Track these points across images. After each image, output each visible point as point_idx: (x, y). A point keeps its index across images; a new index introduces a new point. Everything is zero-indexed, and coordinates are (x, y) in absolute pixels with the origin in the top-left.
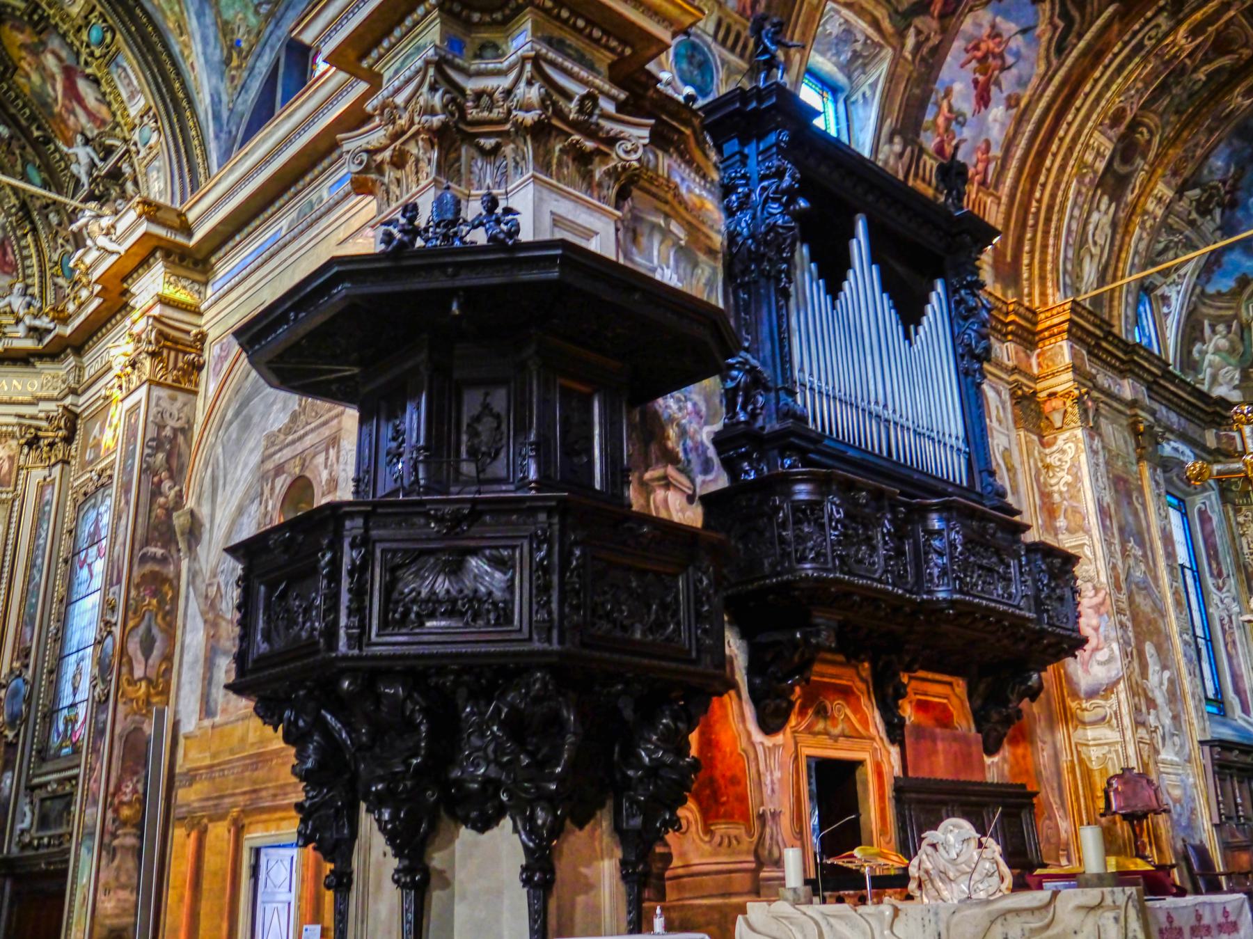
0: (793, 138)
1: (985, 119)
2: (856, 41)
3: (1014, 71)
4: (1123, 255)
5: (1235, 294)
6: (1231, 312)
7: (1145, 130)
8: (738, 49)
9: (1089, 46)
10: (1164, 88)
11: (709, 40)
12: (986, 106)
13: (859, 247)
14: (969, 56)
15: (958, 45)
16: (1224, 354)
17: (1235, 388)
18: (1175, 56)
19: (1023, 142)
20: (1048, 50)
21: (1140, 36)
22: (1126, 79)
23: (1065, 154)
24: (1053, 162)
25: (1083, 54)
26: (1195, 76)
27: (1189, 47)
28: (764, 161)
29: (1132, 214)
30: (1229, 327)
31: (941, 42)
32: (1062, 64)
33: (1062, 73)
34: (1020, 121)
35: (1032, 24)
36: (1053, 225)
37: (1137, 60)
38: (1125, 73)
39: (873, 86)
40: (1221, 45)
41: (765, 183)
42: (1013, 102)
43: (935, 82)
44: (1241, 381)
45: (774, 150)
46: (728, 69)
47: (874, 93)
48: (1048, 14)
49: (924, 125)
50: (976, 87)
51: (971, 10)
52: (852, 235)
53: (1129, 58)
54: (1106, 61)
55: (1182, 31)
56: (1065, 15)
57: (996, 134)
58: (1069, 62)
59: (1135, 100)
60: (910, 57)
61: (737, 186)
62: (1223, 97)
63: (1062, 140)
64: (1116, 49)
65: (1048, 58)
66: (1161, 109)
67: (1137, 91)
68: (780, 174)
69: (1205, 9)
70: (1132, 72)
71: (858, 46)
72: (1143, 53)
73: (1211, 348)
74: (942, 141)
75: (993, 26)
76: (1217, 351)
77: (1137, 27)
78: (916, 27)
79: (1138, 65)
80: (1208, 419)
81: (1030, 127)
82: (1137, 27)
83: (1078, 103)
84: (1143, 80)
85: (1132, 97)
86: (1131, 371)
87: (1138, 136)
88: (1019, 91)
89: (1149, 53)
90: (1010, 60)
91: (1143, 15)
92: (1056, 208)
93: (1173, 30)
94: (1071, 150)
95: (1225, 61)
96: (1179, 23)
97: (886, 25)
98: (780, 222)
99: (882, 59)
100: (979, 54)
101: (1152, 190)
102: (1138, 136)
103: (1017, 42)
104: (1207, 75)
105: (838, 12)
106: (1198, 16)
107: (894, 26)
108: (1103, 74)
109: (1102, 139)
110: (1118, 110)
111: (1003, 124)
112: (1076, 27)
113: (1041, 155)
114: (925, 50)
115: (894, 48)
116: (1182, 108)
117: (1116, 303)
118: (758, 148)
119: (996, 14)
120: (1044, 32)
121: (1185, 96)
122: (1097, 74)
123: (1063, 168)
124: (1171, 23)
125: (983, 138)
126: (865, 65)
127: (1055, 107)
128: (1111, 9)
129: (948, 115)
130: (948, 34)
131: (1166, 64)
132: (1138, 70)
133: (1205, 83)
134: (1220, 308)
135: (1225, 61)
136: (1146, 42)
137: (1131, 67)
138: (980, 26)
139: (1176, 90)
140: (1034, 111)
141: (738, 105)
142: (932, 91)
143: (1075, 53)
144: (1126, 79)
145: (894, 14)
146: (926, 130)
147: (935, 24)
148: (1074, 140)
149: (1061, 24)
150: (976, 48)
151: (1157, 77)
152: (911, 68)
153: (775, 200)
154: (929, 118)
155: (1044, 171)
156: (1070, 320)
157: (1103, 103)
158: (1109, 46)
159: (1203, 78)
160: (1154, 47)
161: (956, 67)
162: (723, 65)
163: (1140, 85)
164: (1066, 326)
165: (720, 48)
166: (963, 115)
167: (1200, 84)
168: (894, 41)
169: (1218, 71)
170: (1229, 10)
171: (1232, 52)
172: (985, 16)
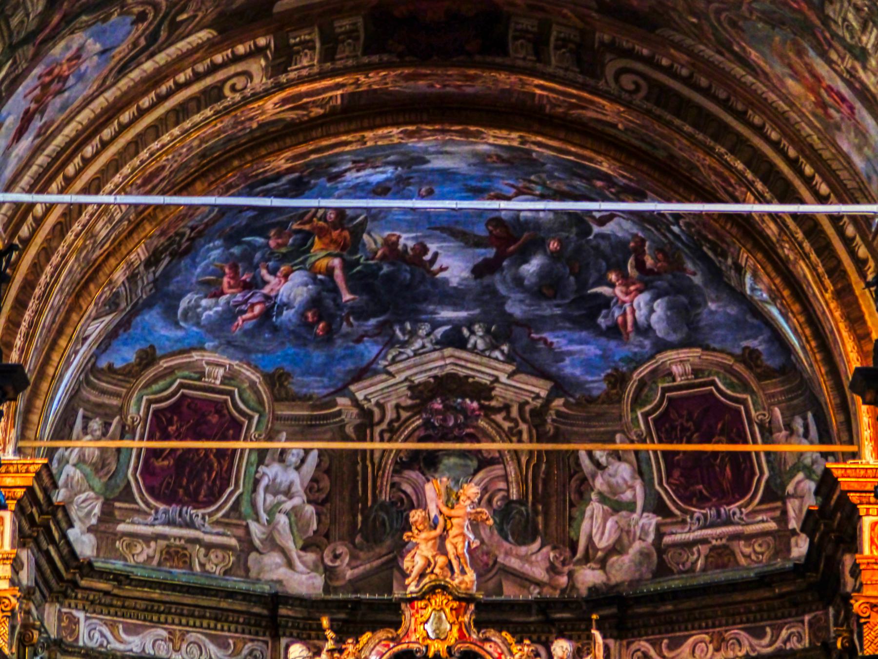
4: (63, 342)
5: (130, 374)
6: (115, 402)
15: (37, 71)
16: (88, 470)
17: (90, 530)
21: (220, 76)
29: (91, 279)
30: (107, 425)
32: (114, 84)
34: (36, 151)
36: (27, 316)
37: (208, 112)
38: (187, 124)
44: (100, 520)
54: (163, 89)
55: (277, 98)
64: (181, 78)
72: (219, 106)
73: (73, 458)
75: (81, 48)
76: (81, 460)
77: (219, 58)
80: (53, 582)
81: (42, 159)
82: (219, 58)
86: (36, 541)
89: (227, 111)
91: (232, 46)
92: (37, 291)
93: (267, 93)
96: (280, 87)
101: (129, 253)
106: (304, 88)
108: (153, 106)
117: (35, 418)
128: (204, 35)
134: (103, 392)
136: (227, 91)
137: (197, 118)
149: (143, 42)
156: (30, 490)
157: (144, 154)
160: (236, 106)
164: (20, 493)
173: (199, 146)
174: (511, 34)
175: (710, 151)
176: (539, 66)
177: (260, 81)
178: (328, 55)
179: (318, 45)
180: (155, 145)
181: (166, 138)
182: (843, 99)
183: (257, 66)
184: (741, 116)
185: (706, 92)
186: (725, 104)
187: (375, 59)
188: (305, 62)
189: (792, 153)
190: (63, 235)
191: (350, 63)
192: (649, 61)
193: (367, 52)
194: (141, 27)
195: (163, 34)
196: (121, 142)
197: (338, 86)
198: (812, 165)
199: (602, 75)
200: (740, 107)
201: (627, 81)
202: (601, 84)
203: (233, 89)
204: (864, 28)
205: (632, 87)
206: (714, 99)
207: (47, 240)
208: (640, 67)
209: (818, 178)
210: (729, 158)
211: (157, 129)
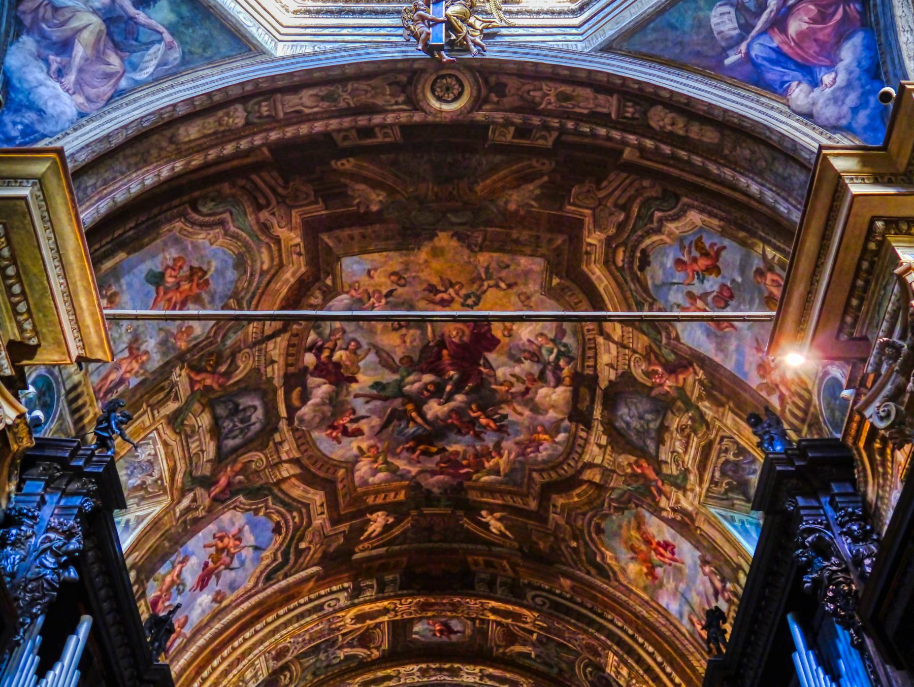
0: (95, 510)
1: (194, 599)
2: (151, 475)
3: (233, 574)
7: (288, 675)
8: (76, 416)
9: (288, 587)
10: (316, 650)
11: (63, 392)
12: (201, 590)
13: (74, 646)
14: (213, 541)
15: (212, 527)
18: (338, 629)
19: (208, 635)
20: (262, 572)
21: (323, 600)
22: (302, 626)
23: (232, 662)
24: (220, 664)
25: (282, 591)
26: (338, 652)
27: (350, 627)
28: (59, 516)
31: (203, 517)
32: (264, 590)
33: (261, 596)
34: (216, 615)
35: (263, 546)
37: (315, 616)
38: (303, 622)
39: (140, 519)
40: (365, 640)
41: (52, 535)
42: (219, 598)
43: (181, 546)
45: (76, 511)
46: (61, 425)
47: (138, 524)
48: (277, 545)
49: (156, 575)
50: (204, 569)
51: (234, 508)
52: (74, 631)
53: (310, 612)
54: (292, 606)
56: (286, 555)
57: (196, 616)
58: (269, 591)
59: (298, 647)
60: (178, 514)
61: (22, 524)
62: (348, 679)
63: (234, 649)
64: (302, 601)
65: (258, 578)
66: (307, 664)
67: (304, 640)
68: (69, 535)
69: (373, 605)
70: (308, 623)
71: (149, 480)
72: (320, 614)
74: (159, 597)
75: (240, 530)
77: (322, 592)
78: (195, 494)
79: (313, 621)
81: (218, 626)
82: (322, 592)
83: (258, 627)
84: (311, 635)
85: (298, 643)
87: (282, 677)
88: (228, 592)
89: (325, 616)
90: (236, 563)
94: (238, 660)
95: (361, 652)
96: (354, 605)
97: (179, 477)
98: (49, 577)
99: (160, 502)
100: (220, 545)
102: (282, 677)
103: (248, 553)
104: (346, 657)
105: (155, 443)
107: (183, 483)
108: (285, 614)
109: (264, 665)
110: (285, 647)
111: (203, 611)
112: (286, 568)
113: (215, 653)
114: (190, 517)
115: (173, 500)
116: (318, 673)
118: (58, 502)
119: (247, 523)
120: (267, 557)
121: (325, 664)
122: (281, 612)
123: (226, 673)
124: (349, 603)
125: (186, 613)
126: (143, 498)
127: (244, 620)
129: (175, 578)
130: (212, 514)
131: (332, 631)
132: (313, 625)
133: (341, 662)
135: (361, 652)
136: (326, 607)
137: (308, 619)
138: (233, 524)
139: (322, 656)
140: (227, 614)
141: (67, 455)
142: (176, 550)
143: (276, 587)
144: (302, 626)
145: (189, 473)
146: (155, 580)
147: (207, 502)
148: (243, 655)
149: (280, 560)
150: (221, 539)
151: (320, 638)
152: (174, 523)
153: (56, 555)
154: (162, 571)
155: (209, 668)
157: (277, 636)
158: (298, 595)
159: (342, 657)
160: (331, 613)
161: (201, 545)
162: (59, 419)
163: (307, 637)
165: (65, 404)
166: (184, 585)
167: (338, 660)
168: (176, 494)
169: (355, 657)
170: (385, 615)
171: (368, 648)
172: (240, 519)
173: (310, 641)
174: (476, 581)
175: (586, 632)
176: (492, 594)
177: (343, 602)
178: (381, 590)
179: (375, 586)
180: (284, 632)
181: (290, 628)
182: (666, 545)
183: (342, 596)
184: (601, 615)
185: (581, 605)
186: (591, 610)
187: (405, 592)
188: (368, 594)
189: (630, 632)
190: (226, 676)
191: (392, 594)
192: (550, 591)
193: (401, 588)
194: (280, 539)
195: (292, 557)
196: (266, 630)
197: (386, 611)
198: (643, 638)
199: (525, 597)
200: (599, 611)
201: (539, 600)
202: (525, 602)
203: (329, 606)
204: (685, 452)
205: (541, 603)
206: (586, 608)
207: (217, 679)
208: (544, 594)
209: (646, 644)
210: (597, 634)
211: (286, 625)
